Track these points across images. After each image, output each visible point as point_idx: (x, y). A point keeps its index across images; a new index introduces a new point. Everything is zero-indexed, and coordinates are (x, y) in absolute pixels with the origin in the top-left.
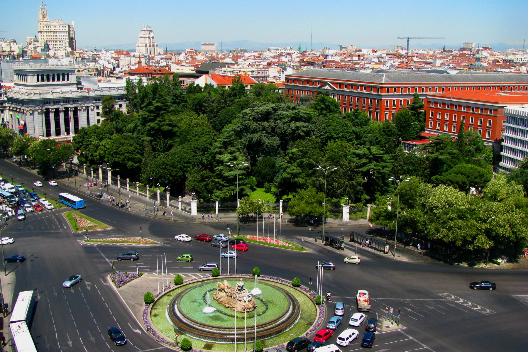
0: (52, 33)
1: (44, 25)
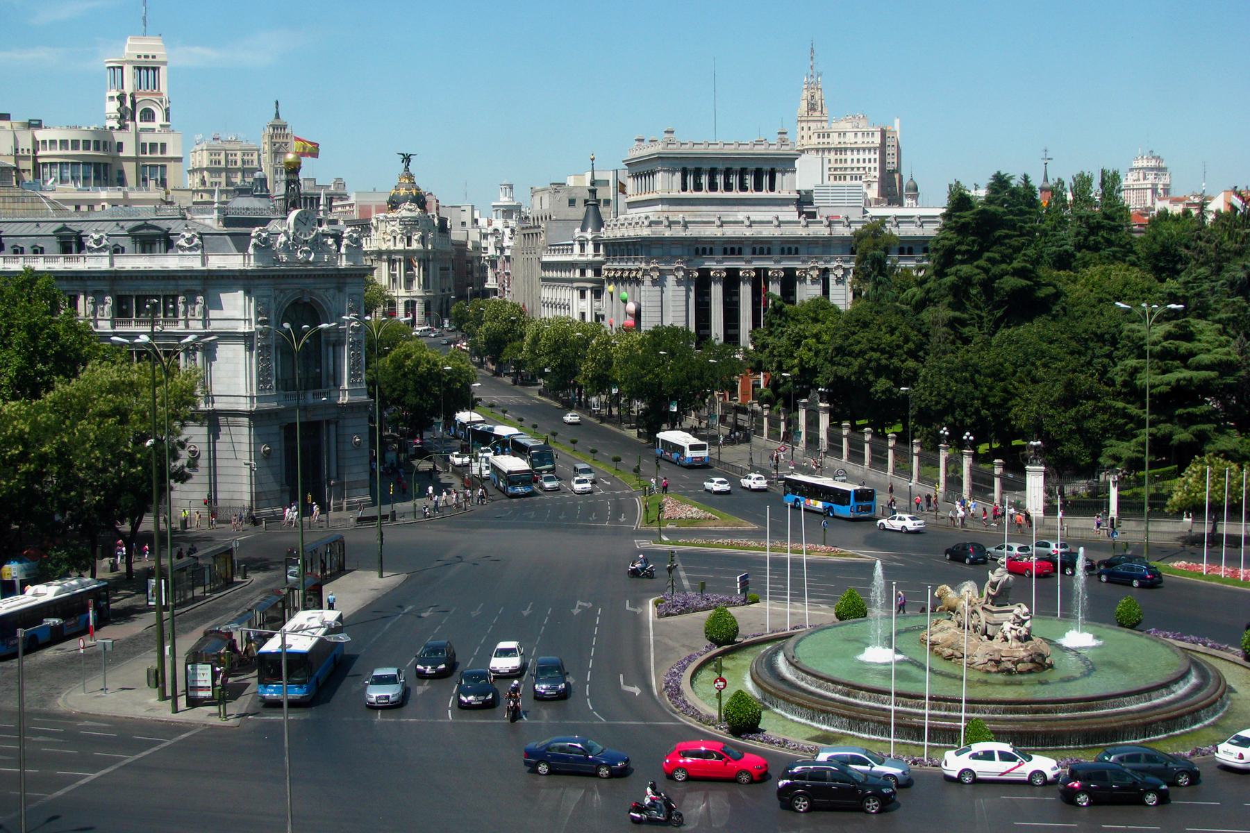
0: (833, 153)
1: (811, 133)
